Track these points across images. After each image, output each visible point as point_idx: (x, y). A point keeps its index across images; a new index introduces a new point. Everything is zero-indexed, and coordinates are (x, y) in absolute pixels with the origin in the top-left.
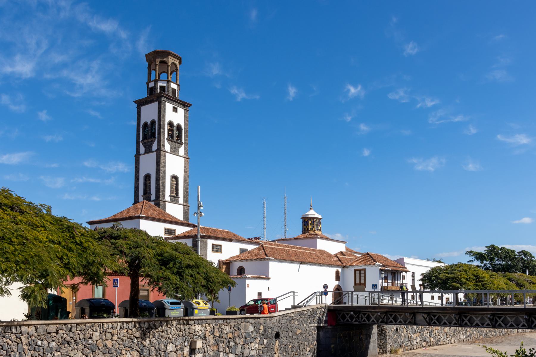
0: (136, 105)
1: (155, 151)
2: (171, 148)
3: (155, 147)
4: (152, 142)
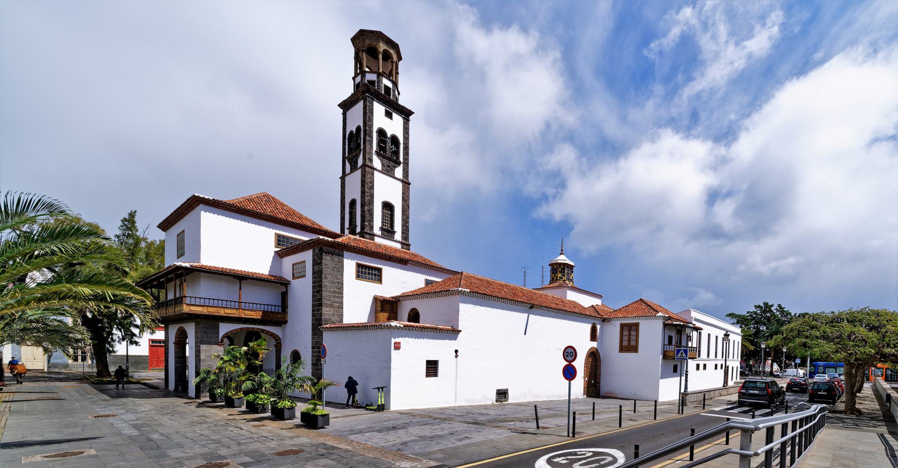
0: (341, 111)
1: (361, 167)
2: (383, 165)
3: (360, 162)
4: (357, 156)
